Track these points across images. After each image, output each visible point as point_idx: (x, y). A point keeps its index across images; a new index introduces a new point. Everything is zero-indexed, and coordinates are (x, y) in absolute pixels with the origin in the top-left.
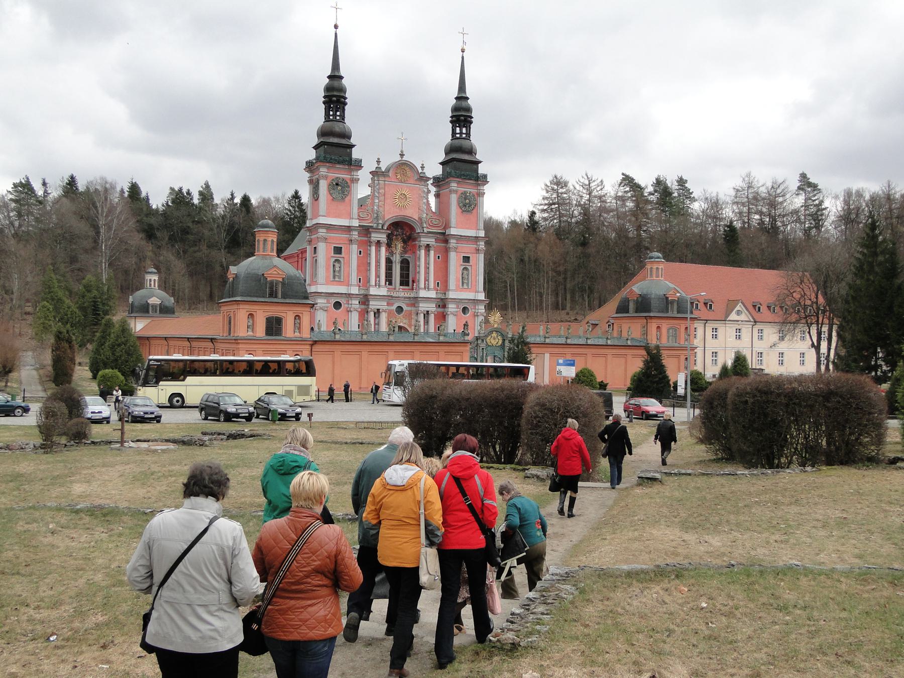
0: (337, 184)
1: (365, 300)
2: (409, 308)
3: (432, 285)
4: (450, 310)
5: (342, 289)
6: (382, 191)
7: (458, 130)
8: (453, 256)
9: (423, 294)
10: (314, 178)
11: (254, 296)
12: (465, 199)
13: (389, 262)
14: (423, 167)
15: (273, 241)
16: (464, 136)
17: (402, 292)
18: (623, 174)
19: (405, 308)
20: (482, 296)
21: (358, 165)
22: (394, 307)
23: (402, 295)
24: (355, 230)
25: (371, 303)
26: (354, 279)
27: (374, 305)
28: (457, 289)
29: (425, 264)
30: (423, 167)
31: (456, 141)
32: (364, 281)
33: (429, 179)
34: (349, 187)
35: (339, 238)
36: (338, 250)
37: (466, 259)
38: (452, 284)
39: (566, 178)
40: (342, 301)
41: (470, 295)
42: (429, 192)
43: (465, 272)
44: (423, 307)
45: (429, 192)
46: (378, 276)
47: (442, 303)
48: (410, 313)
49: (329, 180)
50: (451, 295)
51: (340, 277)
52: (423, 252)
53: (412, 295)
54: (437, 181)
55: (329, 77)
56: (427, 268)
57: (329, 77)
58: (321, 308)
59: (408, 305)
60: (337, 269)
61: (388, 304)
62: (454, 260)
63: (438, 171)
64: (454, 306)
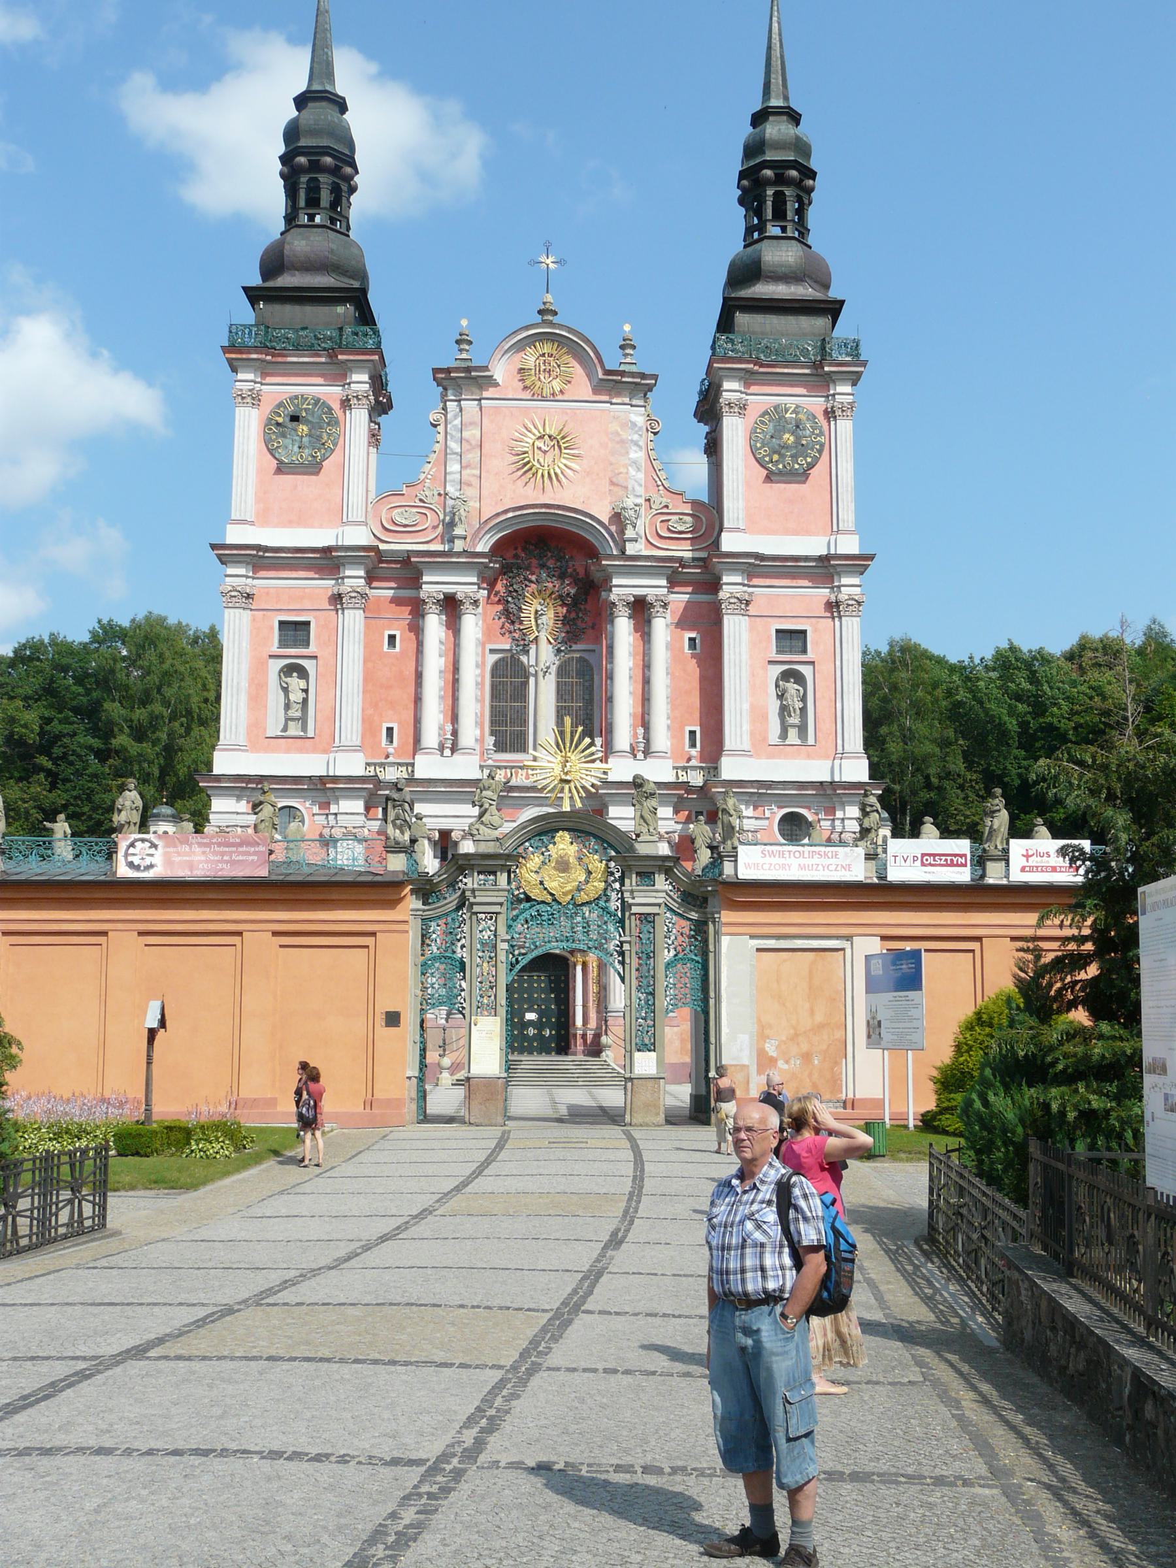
0: (295, 418)
3: (662, 739)
5: (310, 765)
6: (472, 433)
8: (734, 628)
16: (776, 231)
20: (857, 770)
24: (355, 561)
26: (350, 728)
35: (304, 593)
38: (736, 731)
41: (817, 771)
49: (267, 407)
50: (730, 769)
62: (744, 643)
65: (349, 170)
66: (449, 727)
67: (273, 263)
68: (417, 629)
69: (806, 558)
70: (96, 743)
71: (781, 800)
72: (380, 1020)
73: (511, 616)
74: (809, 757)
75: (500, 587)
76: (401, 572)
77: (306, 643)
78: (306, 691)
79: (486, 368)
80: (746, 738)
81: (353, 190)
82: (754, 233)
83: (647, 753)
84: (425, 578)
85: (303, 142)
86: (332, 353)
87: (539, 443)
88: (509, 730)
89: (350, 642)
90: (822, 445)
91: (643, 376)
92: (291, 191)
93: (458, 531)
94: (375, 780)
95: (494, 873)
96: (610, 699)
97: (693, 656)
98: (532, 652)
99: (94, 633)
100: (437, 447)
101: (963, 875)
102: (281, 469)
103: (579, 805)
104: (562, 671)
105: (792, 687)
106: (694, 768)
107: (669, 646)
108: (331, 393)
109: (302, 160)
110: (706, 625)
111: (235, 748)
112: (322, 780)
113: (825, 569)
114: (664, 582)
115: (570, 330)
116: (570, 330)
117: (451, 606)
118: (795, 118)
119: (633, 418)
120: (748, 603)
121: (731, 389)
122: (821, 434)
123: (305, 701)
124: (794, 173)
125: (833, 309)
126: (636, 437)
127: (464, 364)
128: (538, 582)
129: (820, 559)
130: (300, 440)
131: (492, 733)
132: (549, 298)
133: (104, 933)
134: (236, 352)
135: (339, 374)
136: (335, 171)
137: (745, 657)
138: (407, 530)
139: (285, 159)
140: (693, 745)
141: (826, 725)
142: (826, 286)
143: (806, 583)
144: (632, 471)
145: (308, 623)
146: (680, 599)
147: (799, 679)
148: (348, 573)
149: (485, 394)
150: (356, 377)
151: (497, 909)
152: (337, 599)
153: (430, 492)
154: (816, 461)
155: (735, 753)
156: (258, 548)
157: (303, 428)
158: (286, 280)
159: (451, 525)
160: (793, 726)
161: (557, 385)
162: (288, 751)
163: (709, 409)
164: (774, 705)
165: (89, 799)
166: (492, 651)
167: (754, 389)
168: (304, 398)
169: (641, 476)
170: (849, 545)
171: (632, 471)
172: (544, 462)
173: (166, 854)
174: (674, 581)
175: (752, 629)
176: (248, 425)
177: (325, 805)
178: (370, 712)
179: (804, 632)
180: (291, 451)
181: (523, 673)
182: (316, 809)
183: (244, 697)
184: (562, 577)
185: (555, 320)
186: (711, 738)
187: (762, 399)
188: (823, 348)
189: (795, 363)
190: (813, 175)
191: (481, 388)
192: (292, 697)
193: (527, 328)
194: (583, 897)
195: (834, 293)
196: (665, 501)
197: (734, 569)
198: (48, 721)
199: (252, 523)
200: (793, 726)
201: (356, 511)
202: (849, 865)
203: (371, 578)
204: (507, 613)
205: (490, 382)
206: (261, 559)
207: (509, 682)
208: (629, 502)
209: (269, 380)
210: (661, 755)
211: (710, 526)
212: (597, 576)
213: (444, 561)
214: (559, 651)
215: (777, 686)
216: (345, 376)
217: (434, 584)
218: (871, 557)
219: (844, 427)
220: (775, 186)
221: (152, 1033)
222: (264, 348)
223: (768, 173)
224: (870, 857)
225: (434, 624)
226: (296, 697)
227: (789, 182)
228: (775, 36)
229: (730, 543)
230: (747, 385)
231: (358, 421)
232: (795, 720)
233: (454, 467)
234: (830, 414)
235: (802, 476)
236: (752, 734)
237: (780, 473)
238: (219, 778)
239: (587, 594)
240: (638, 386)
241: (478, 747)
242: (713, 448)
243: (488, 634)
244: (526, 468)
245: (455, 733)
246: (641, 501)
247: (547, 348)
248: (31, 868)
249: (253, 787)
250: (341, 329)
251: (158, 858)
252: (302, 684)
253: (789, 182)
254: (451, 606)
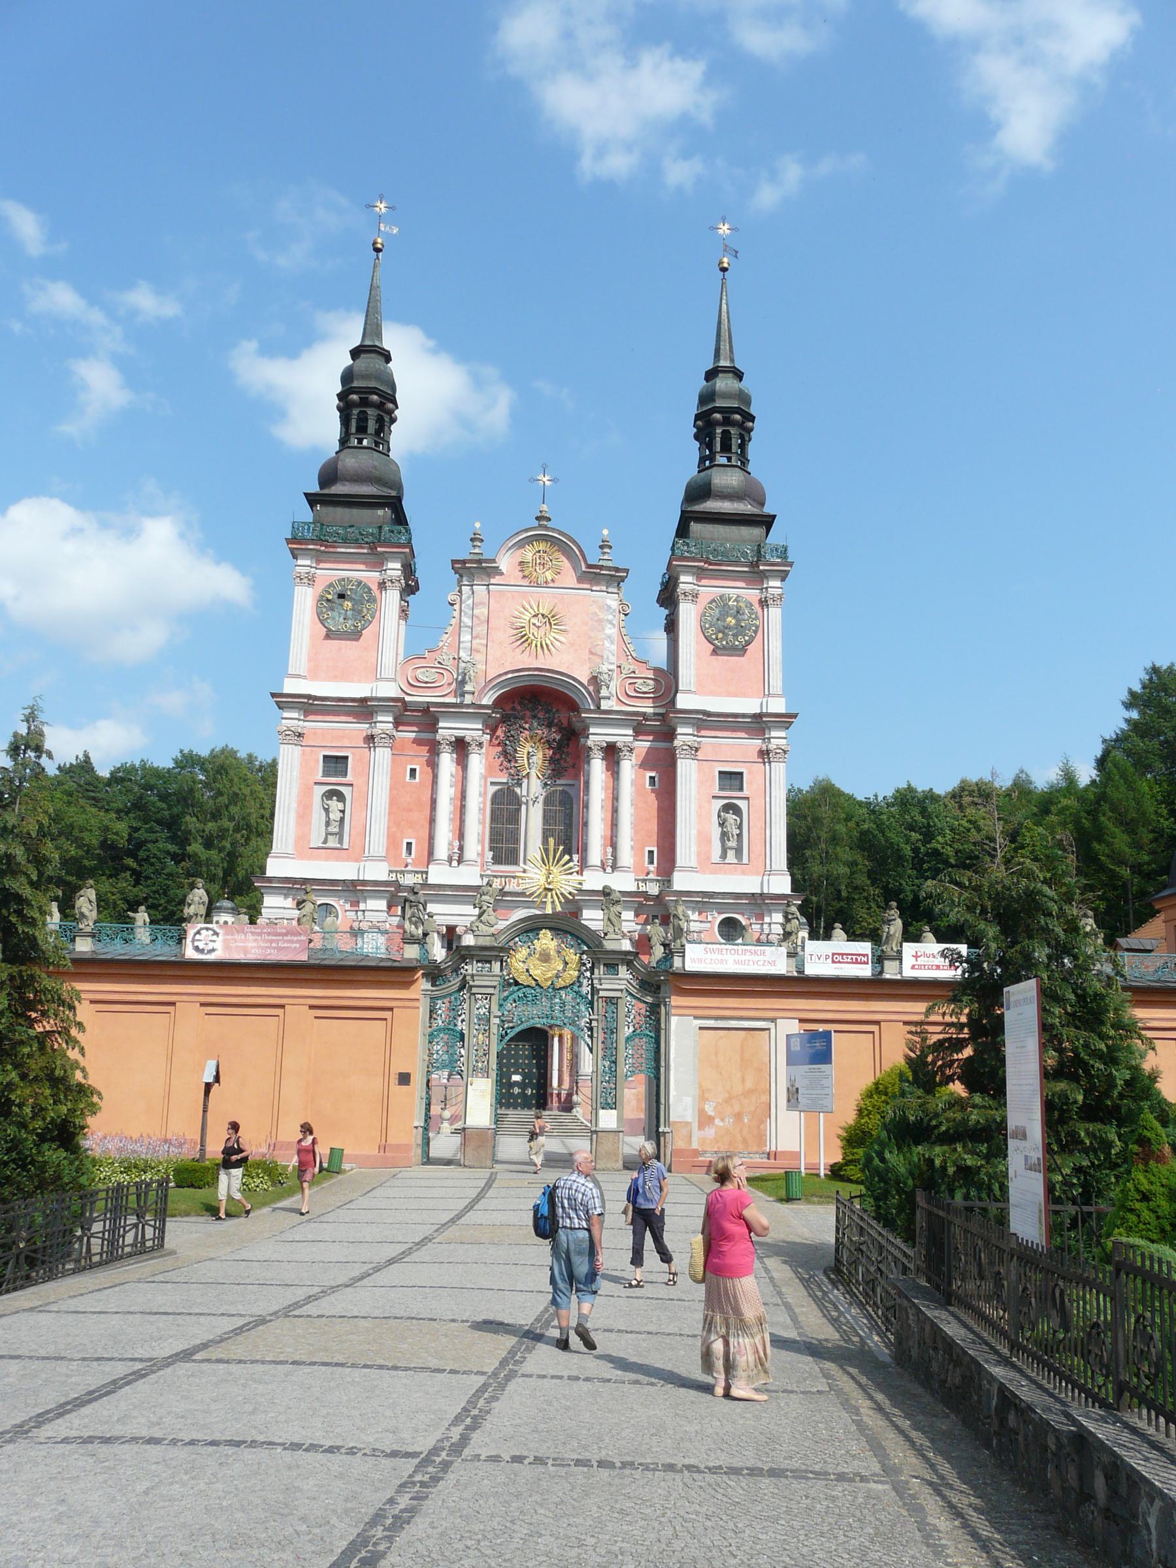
0: (342, 596)
3: (626, 856)
5: (344, 871)
8: (686, 769)
16: (724, 461)
20: (782, 884)
24: (385, 710)
26: (377, 842)
28: (705, 863)
34: (372, 600)
35: (344, 734)
38: (686, 851)
41: (749, 884)
49: (320, 587)
50: (681, 882)
62: (693, 782)
65: (391, 406)
66: (457, 843)
67: (329, 475)
68: (433, 764)
69: (744, 716)
70: (172, 848)
71: (721, 908)
72: (394, 1079)
73: (508, 756)
74: (743, 873)
75: (499, 732)
76: (421, 719)
78: (343, 812)
79: (494, 561)
80: (694, 857)
81: (393, 420)
82: (706, 462)
83: (614, 867)
84: (441, 725)
85: (355, 384)
86: (373, 547)
87: (534, 620)
88: (505, 846)
89: (379, 773)
90: (757, 627)
91: (617, 570)
92: (345, 421)
93: (468, 688)
94: (396, 884)
95: (490, 962)
96: (586, 824)
97: (653, 791)
98: (525, 785)
99: (176, 761)
100: (453, 621)
101: (866, 971)
102: (329, 635)
103: (559, 909)
104: (548, 801)
105: (731, 817)
106: (651, 880)
107: (633, 783)
108: (371, 577)
109: (355, 397)
110: (663, 766)
111: (286, 856)
112: (354, 883)
113: (758, 724)
114: (631, 732)
115: (560, 533)
116: (560, 533)
117: (461, 746)
118: (739, 375)
119: (609, 602)
120: (697, 750)
121: (686, 581)
122: (757, 618)
123: (342, 820)
124: (738, 417)
125: (767, 522)
126: (610, 617)
127: (476, 557)
128: (530, 729)
129: (755, 716)
130: (346, 613)
131: (491, 849)
132: (545, 507)
133: (173, 1004)
134: (297, 543)
135: (378, 563)
136: (380, 406)
137: (693, 793)
138: (427, 686)
139: (341, 396)
140: (651, 862)
141: (757, 848)
142: (763, 504)
143: (743, 735)
144: (607, 644)
145: (346, 758)
146: (643, 745)
147: (737, 811)
148: (380, 718)
149: (493, 581)
150: (390, 565)
151: (491, 991)
152: (370, 739)
153: (447, 658)
154: (752, 639)
156: (309, 697)
157: (348, 604)
158: (338, 489)
159: (463, 683)
160: (731, 848)
161: (549, 575)
162: (327, 859)
163: (668, 597)
164: (716, 832)
165: (165, 893)
166: (492, 783)
167: (704, 582)
168: (349, 580)
169: (614, 647)
170: (777, 706)
171: (607, 644)
172: (538, 634)
173: (225, 941)
174: (639, 731)
175: (699, 770)
176: (305, 600)
177: (355, 904)
178: (394, 829)
179: (741, 774)
180: (337, 622)
181: (516, 801)
182: (348, 907)
183: (293, 815)
184: (549, 726)
185: (549, 524)
186: (666, 856)
187: (710, 590)
188: (759, 552)
189: (737, 563)
190: (752, 418)
191: (489, 576)
192: (332, 816)
193: (527, 530)
194: (560, 983)
195: (768, 510)
196: (632, 668)
197: (686, 722)
198: (136, 830)
199: (305, 677)
200: (731, 848)
201: (388, 669)
202: (773, 961)
203: (397, 723)
204: (505, 753)
205: (497, 571)
206: (310, 706)
207: (505, 808)
208: (604, 668)
209: (322, 565)
210: (625, 869)
211: (668, 689)
212: (578, 726)
213: (456, 711)
214: (546, 784)
215: (719, 816)
216: (382, 564)
217: (448, 729)
218: (795, 716)
219: (775, 614)
220: (722, 426)
221: (208, 1087)
222: (319, 540)
223: (718, 416)
224: (791, 955)
225: (447, 761)
226: (335, 816)
227: (734, 424)
228: (724, 314)
229: (683, 702)
230: (699, 579)
231: (391, 599)
232: (732, 843)
233: (466, 637)
234: (764, 603)
235: (741, 651)
236: (699, 854)
237: (724, 648)
238: (270, 880)
239: (569, 740)
240: (614, 578)
241: (479, 860)
242: (671, 627)
243: (489, 769)
244: (523, 639)
245: (461, 848)
246: (613, 667)
247: (542, 546)
248: (116, 949)
249: (298, 887)
250: (380, 528)
251: (218, 945)
252: (340, 806)
253: (734, 424)
254: (461, 746)
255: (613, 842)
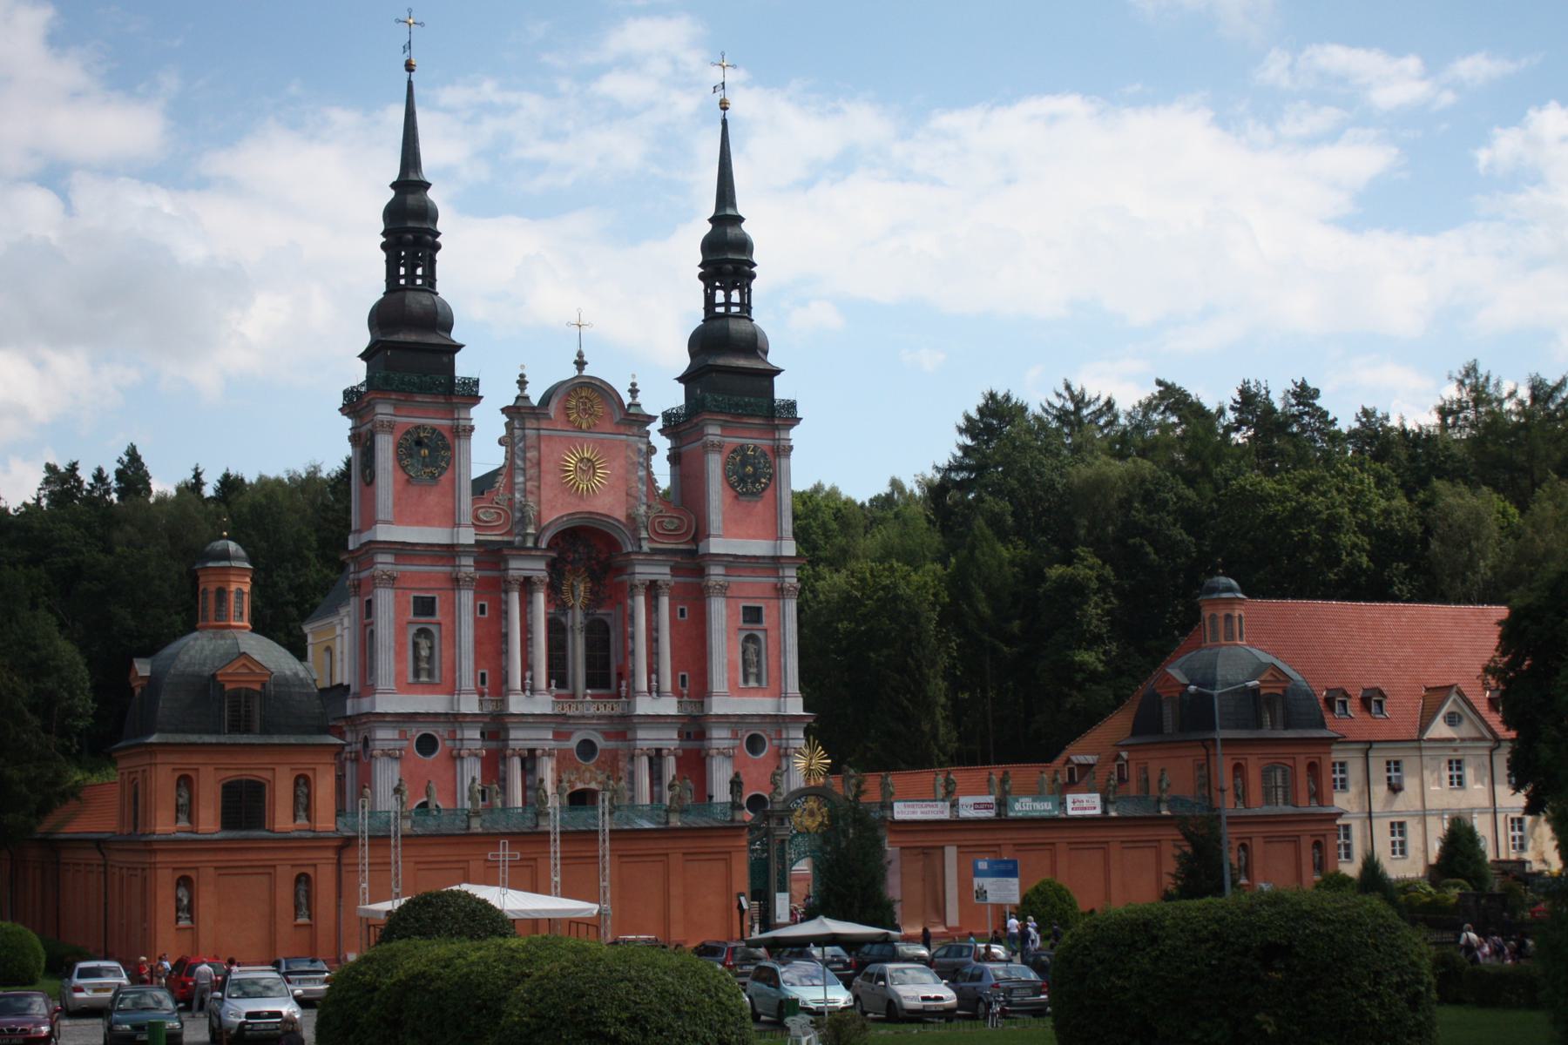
0: (419, 443)
1: (496, 726)
2: (612, 744)
4: (715, 744)
5: (435, 703)
6: (532, 454)
7: (720, 296)
9: (645, 706)
10: (364, 429)
11: (193, 732)
12: (744, 464)
13: (556, 629)
14: (634, 391)
15: (240, 592)
17: (589, 705)
18: (1159, 383)
19: (600, 742)
21: (470, 394)
22: (573, 743)
23: (592, 710)
24: (467, 554)
25: (513, 734)
27: (519, 738)
28: (734, 690)
29: (648, 627)
30: (634, 391)
31: (717, 323)
32: (495, 683)
33: (652, 419)
34: (448, 448)
36: (425, 607)
37: (753, 615)
39: (1018, 396)
40: (439, 732)
42: (652, 450)
43: (752, 647)
44: (646, 738)
45: (652, 450)
46: (527, 665)
47: (694, 727)
48: (614, 757)
51: (430, 674)
52: (641, 601)
53: (618, 711)
54: (674, 425)
55: (394, 186)
56: (653, 640)
57: (394, 186)
58: (388, 754)
59: (607, 736)
60: (424, 653)
61: (558, 736)
62: (721, 615)
63: (676, 397)
64: (725, 733)
77: (432, 613)
88: (558, 672)
117: (527, 586)
140: (683, 685)
155: (719, 694)
157: (425, 452)
213: (521, 551)
233: (520, 479)
255: (653, 669)
